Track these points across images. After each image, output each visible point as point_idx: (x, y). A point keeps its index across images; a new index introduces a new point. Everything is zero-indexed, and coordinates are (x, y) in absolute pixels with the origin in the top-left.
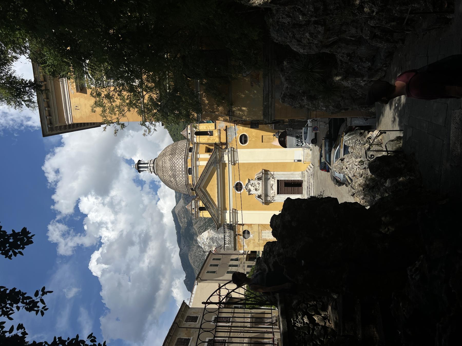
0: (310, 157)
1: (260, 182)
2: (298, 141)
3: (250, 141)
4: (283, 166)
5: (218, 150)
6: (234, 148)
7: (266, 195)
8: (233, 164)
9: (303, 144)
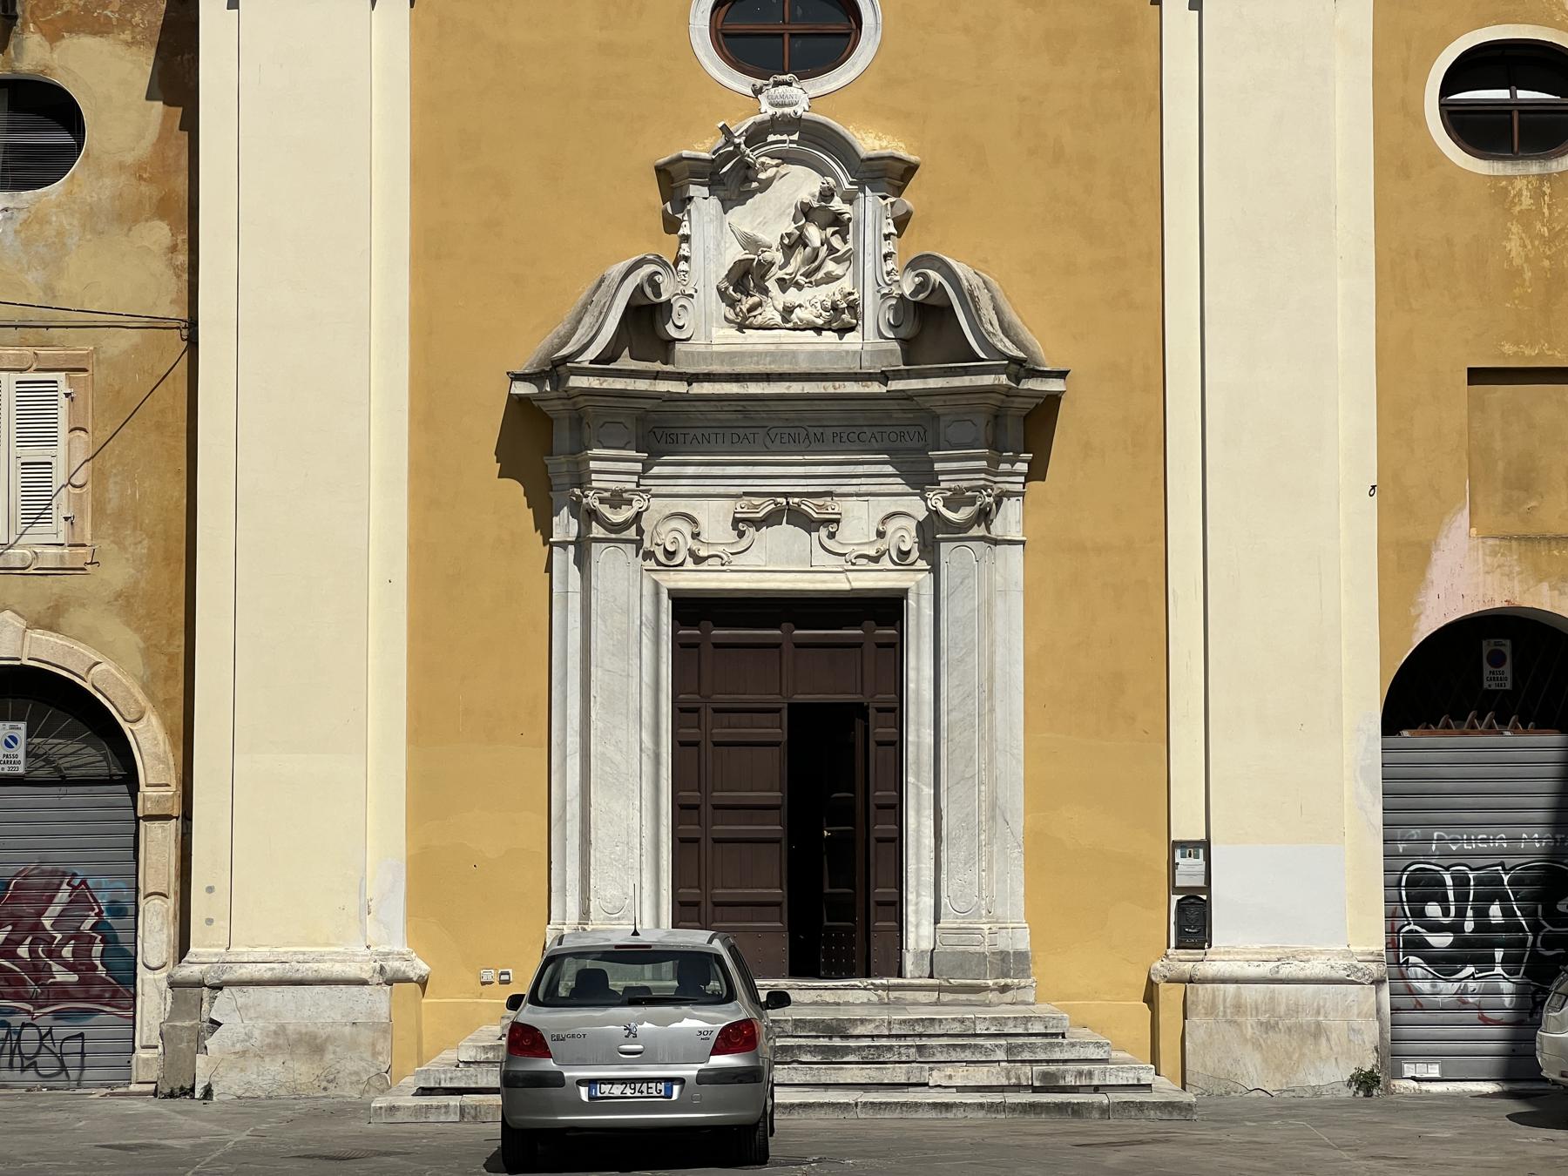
0: (1255, 1073)
1: (870, 341)
2: (1490, 890)
3: (1500, 193)
4: (1113, 685)
7: (663, 431)
9: (1444, 964)
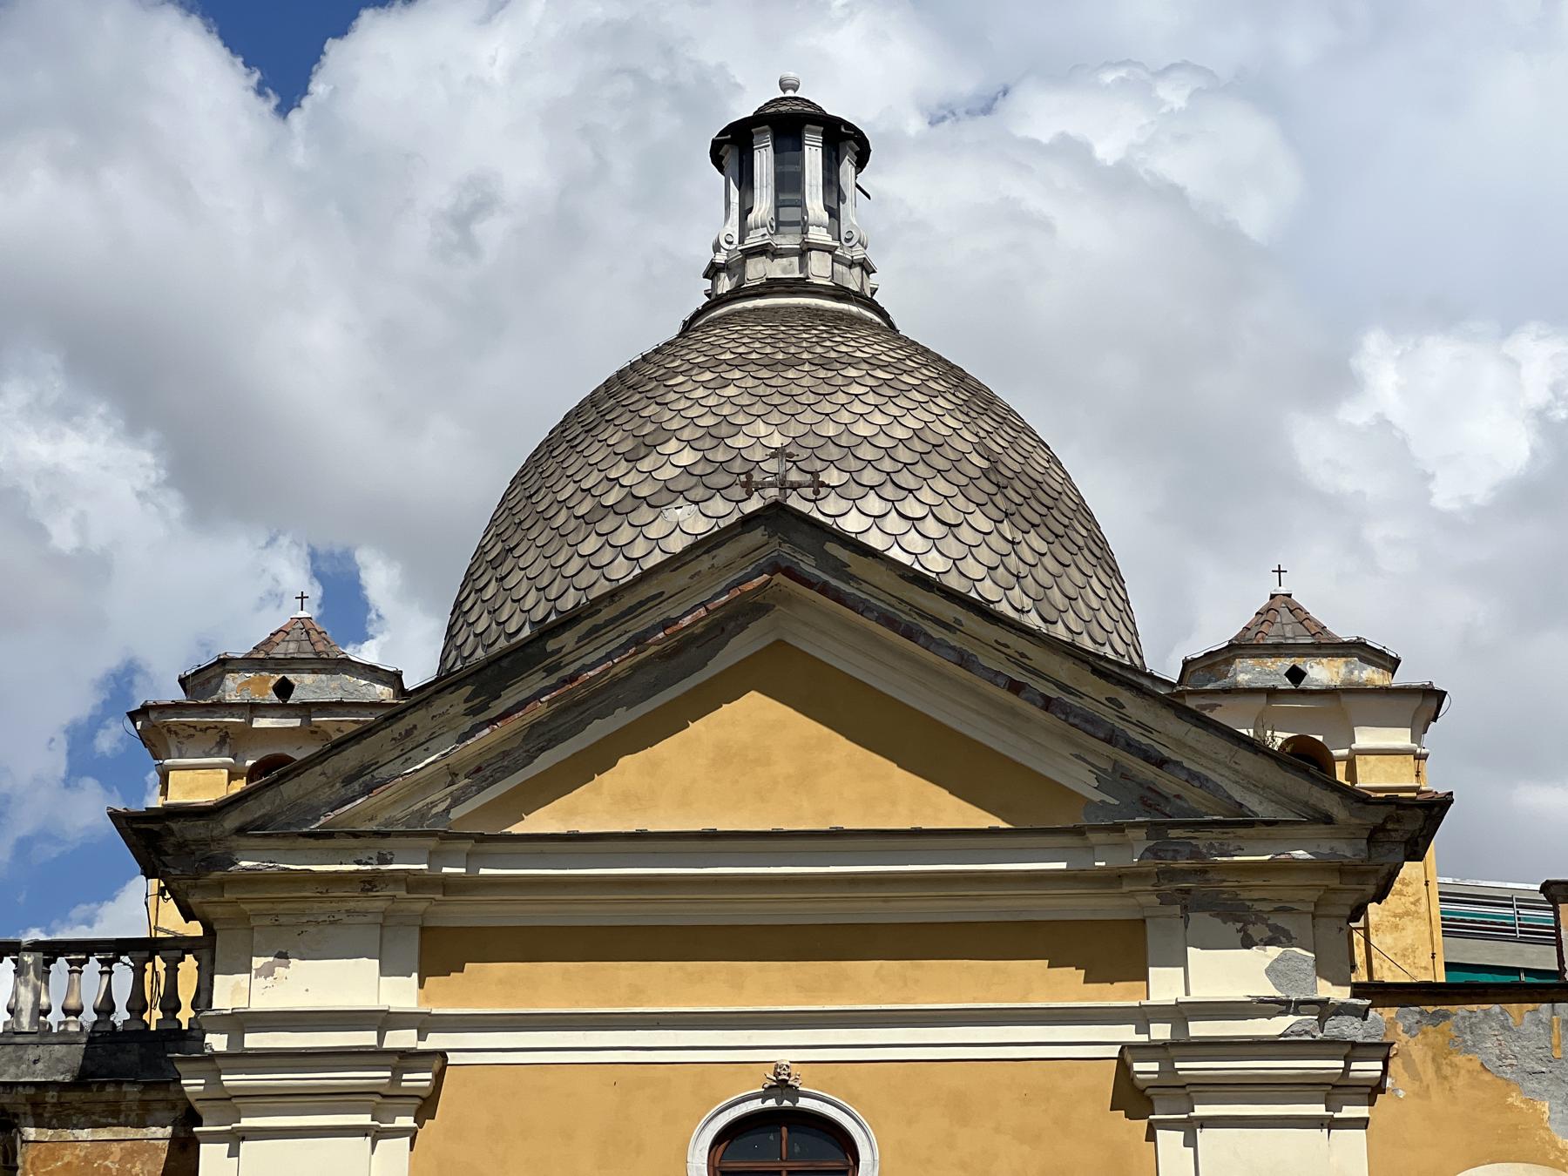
5: (1347, 851)
6: (1373, 1091)
8: (1145, 1068)
